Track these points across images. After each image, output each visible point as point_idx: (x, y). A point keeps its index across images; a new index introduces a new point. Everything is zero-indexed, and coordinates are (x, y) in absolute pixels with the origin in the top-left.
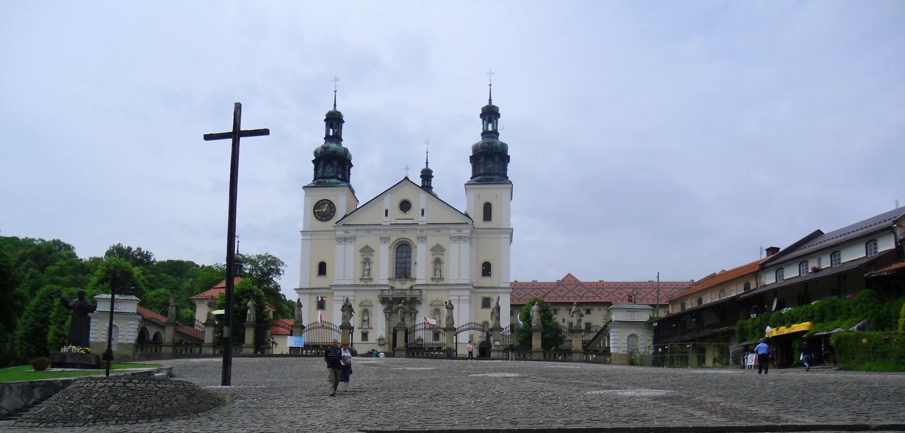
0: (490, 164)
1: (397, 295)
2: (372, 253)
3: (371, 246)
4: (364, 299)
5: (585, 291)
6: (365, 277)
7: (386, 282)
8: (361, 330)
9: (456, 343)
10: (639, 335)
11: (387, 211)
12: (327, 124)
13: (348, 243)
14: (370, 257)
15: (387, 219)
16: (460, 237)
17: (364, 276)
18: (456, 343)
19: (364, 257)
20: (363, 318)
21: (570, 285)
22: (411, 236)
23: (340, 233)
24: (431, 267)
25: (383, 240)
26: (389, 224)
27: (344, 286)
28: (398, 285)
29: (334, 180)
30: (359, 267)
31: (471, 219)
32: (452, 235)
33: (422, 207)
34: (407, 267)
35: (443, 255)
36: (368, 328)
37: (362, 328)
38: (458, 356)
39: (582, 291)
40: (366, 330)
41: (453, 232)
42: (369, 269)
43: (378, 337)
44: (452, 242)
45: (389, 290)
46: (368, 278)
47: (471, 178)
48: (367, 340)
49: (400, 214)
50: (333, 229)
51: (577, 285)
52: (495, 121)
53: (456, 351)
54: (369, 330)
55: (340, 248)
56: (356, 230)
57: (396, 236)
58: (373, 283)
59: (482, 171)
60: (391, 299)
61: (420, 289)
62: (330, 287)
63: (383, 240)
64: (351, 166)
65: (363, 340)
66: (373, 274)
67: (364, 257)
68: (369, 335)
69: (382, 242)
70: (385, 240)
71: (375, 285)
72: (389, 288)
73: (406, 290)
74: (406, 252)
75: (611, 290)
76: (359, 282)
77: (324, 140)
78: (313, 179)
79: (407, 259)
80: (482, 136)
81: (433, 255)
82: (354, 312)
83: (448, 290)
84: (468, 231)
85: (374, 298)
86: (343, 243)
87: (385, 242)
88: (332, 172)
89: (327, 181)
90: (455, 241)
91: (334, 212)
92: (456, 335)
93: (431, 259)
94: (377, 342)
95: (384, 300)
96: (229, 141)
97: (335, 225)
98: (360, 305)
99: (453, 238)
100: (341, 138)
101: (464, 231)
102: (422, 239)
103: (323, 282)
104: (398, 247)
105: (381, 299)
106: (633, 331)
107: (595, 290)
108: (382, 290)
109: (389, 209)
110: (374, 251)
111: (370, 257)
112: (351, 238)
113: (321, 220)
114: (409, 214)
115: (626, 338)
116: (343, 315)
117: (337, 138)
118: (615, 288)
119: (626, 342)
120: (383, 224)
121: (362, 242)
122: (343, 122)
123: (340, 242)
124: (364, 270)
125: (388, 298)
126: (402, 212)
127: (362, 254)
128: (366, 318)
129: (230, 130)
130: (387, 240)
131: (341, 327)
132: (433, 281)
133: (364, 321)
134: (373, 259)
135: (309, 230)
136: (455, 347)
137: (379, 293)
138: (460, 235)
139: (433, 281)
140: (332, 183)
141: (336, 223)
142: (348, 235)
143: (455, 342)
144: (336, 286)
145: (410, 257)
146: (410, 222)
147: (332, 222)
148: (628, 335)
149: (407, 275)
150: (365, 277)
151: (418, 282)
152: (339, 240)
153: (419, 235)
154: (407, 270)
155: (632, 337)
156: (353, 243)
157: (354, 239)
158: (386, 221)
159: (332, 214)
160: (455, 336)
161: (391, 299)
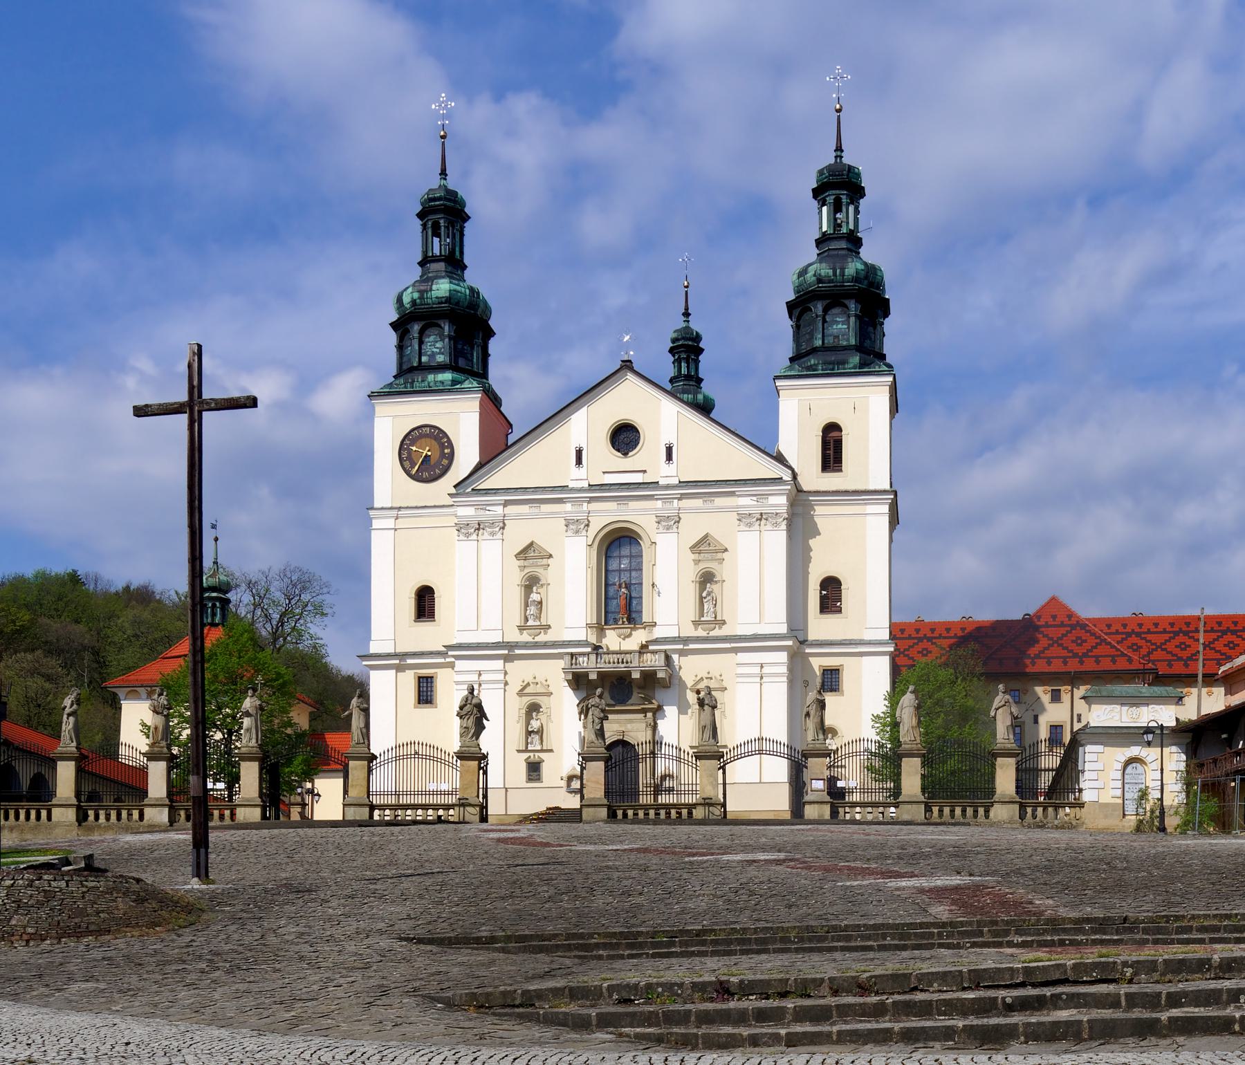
0: (838, 323)
1: (607, 664)
2: (545, 561)
3: (544, 543)
4: (529, 679)
5: (1092, 641)
6: (528, 624)
7: (581, 635)
8: (526, 755)
9: (724, 784)
10: (1148, 760)
11: (579, 453)
12: (424, 226)
13: (486, 536)
14: (540, 570)
15: (581, 472)
16: (761, 514)
17: (527, 620)
18: (724, 784)
19: (526, 571)
20: (528, 724)
21: (1055, 626)
22: (640, 515)
23: (467, 512)
24: (691, 591)
25: (571, 527)
26: (586, 485)
27: (479, 646)
28: (612, 640)
29: (447, 376)
30: (515, 595)
31: (793, 470)
32: (742, 511)
34: (634, 595)
36: (542, 751)
37: (526, 751)
38: (728, 817)
39: (1085, 641)
40: (537, 754)
41: (745, 502)
42: (540, 603)
43: (565, 774)
44: (743, 527)
45: (588, 654)
46: (539, 624)
47: (792, 360)
48: (539, 779)
49: (614, 460)
50: (449, 501)
51: (1073, 627)
52: (851, 208)
53: (724, 805)
54: (543, 755)
55: (464, 549)
56: (506, 504)
57: (605, 515)
59: (818, 343)
60: (593, 676)
61: (665, 651)
62: (444, 649)
63: (571, 527)
64: (490, 333)
65: (530, 779)
66: (549, 616)
67: (526, 571)
68: (545, 769)
69: (570, 533)
70: (576, 525)
71: (554, 645)
72: (589, 650)
73: (630, 652)
74: (631, 556)
75: (1158, 639)
77: (420, 269)
78: (395, 373)
79: (634, 574)
80: (817, 246)
81: (697, 562)
82: (488, 720)
83: (736, 651)
84: (783, 500)
85: (553, 673)
86: (474, 537)
88: (440, 353)
89: (431, 377)
90: (750, 525)
91: (451, 457)
92: (723, 768)
93: (691, 573)
94: (563, 783)
95: (578, 681)
96: (183, 419)
97: (453, 491)
98: (521, 693)
100: (462, 260)
101: (773, 500)
102: (670, 522)
103: (428, 637)
105: (570, 677)
106: (1135, 751)
107: (1119, 637)
108: (572, 655)
109: (584, 446)
110: (551, 556)
111: (540, 570)
113: (417, 478)
114: (637, 459)
115: (1119, 766)
116: (461, 726)
117: (455, 264)
118: (1170, 632)
119: (1119, 775)
120: (572, 485)
121: (519, 535)
122: (466, 218)
123: (468, 535)
124: (527, 605)
125: (587, 674)
126: (619, 454)
127: (521, 563)
128: (535, 724)
129: (183, 397)
130: (582, 526)
131: (461, 756)
132: (696, 629)
133: (529, 733)
134: (549, 576)
135: (390, 506)
136: (721, 796)
137: (561, 664)
138: (764, 510)
139: (696, 629)
140: (442, 382)
141: (455, 487)
142: (484, 516)
143: (720, 781)
144: (460, 647)
145: (640, 570)
146: (638, 478)
147: (446, 484)
148: (1123, 759)
149: (634, 615)
150: (530, 623)
151: (658, 633)
152: (463, 528)
153: (660, 513)
154: (634, 602)
155: (1134, 765)
156: (499, 536)
158: (577, 477)
159: (445, 462)
160: (721, 771)
161: (593, 676)
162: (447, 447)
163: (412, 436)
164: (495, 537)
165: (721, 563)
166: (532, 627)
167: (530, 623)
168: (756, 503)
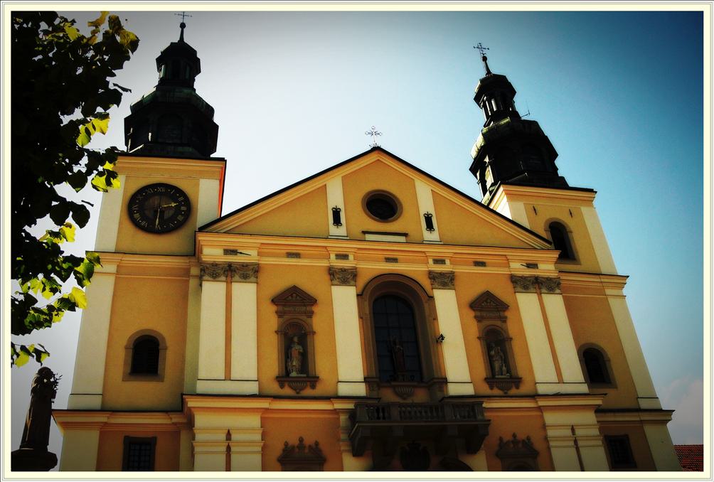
14: (304, 318)
15: (341, 231)
19: (286, 317)
33: (423, 211)
35: (504, 320)
55: (213, 291)
58: (319, 391)
69: (335, 282)
70: (343, 276)
76: (274, 388)
87: (345, 282)
99: (521, 283)
102: (446, 280)
104: (376, 300)
109: (341, 206)
111: (304, 318)
112: (244, 266)
157: (249, 272)
159: (180, 218)
162: (184, 205)
163: (146, 193)
164: (248, 280)
165: (505, 322)
166: (296, 380)
167: (294, 374)
168: (525, 268)
